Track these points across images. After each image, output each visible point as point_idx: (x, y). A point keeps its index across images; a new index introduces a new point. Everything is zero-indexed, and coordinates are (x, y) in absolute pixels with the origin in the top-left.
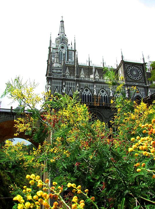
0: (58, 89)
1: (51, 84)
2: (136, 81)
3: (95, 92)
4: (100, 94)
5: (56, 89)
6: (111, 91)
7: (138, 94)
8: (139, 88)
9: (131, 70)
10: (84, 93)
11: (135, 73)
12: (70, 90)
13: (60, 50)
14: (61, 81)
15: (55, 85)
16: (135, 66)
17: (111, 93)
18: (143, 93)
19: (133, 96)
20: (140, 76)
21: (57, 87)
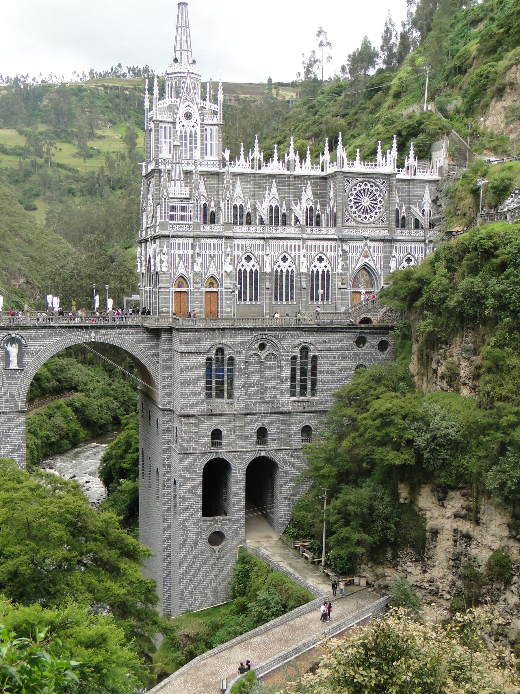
0: (184, 263)
1: (168, 250)
2: (365, 226)
3: (267, 265)
4: (279, 266)
5: (179, 262)
6: (302, 259)
7: (366, 260)
8: (371, 244)
9: (359, 194)
10: (243, 266)
11: (366, 201)
12: (210, 263)
13: (183, 126)
14: (190, 241)
15: (177, 252)
16: (370, 182)
17: (304, 265)
18: (379, 254)
19: (353, 266)
20: (380, 208)
21: (181, 257)
